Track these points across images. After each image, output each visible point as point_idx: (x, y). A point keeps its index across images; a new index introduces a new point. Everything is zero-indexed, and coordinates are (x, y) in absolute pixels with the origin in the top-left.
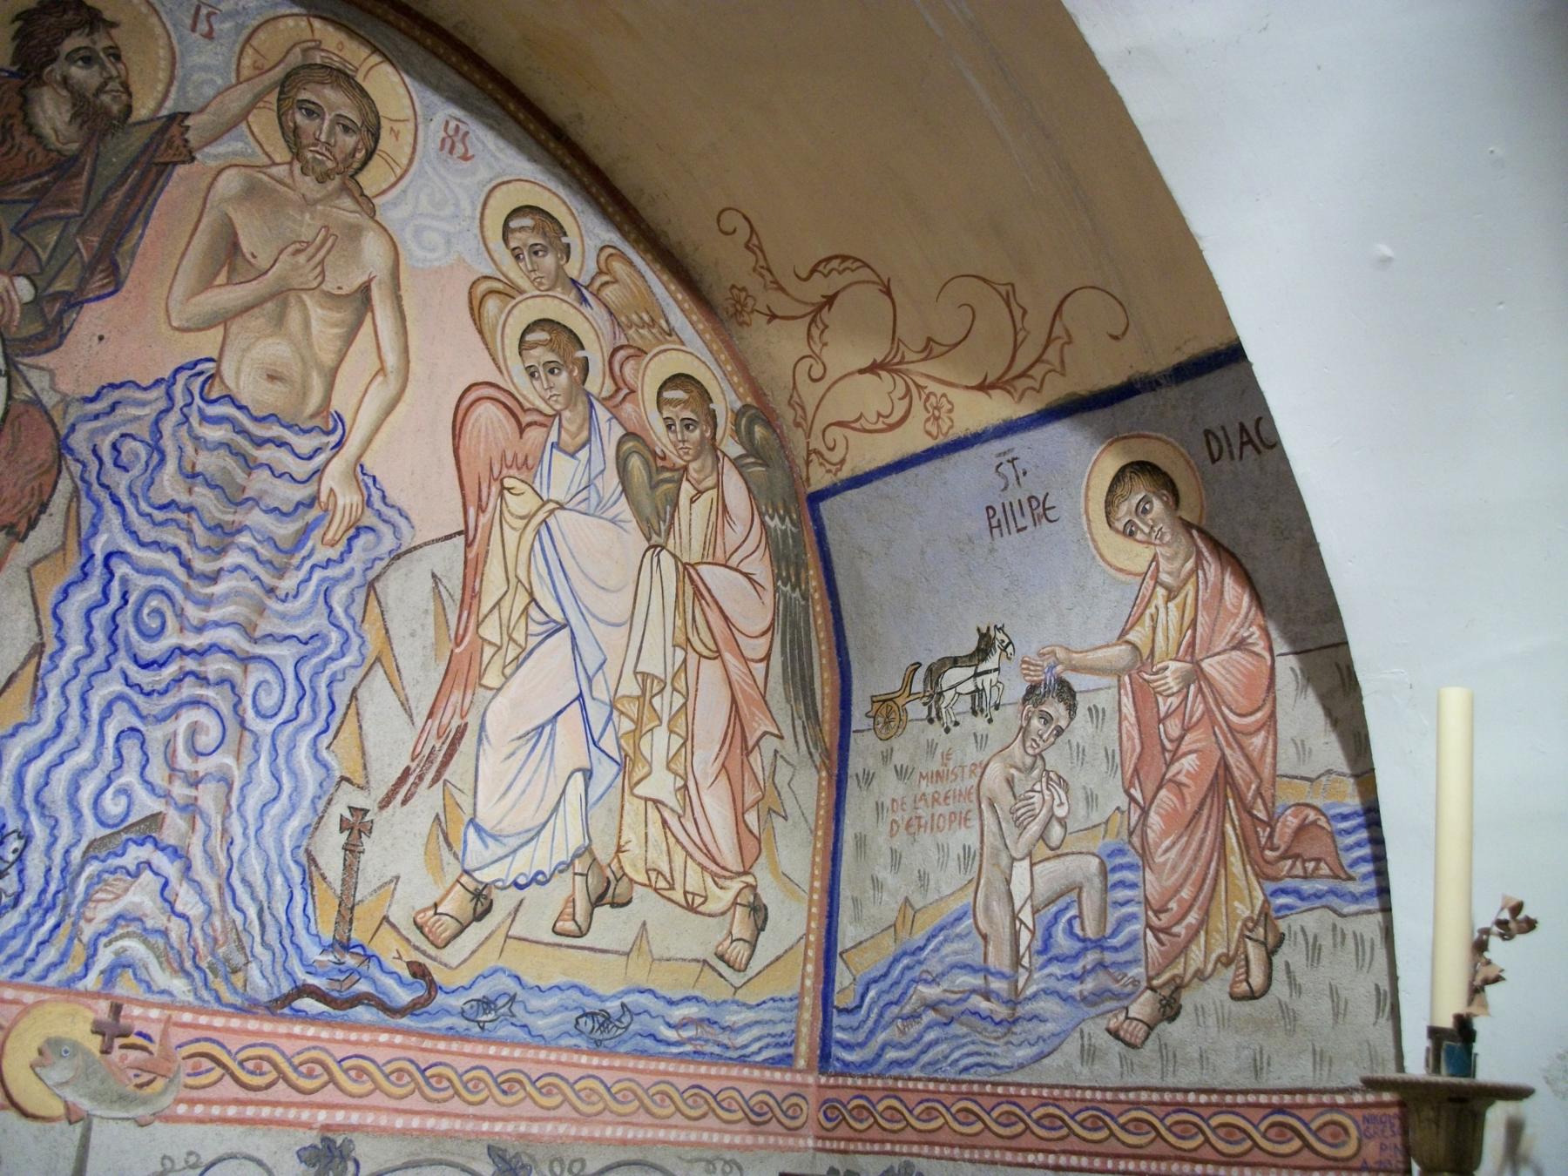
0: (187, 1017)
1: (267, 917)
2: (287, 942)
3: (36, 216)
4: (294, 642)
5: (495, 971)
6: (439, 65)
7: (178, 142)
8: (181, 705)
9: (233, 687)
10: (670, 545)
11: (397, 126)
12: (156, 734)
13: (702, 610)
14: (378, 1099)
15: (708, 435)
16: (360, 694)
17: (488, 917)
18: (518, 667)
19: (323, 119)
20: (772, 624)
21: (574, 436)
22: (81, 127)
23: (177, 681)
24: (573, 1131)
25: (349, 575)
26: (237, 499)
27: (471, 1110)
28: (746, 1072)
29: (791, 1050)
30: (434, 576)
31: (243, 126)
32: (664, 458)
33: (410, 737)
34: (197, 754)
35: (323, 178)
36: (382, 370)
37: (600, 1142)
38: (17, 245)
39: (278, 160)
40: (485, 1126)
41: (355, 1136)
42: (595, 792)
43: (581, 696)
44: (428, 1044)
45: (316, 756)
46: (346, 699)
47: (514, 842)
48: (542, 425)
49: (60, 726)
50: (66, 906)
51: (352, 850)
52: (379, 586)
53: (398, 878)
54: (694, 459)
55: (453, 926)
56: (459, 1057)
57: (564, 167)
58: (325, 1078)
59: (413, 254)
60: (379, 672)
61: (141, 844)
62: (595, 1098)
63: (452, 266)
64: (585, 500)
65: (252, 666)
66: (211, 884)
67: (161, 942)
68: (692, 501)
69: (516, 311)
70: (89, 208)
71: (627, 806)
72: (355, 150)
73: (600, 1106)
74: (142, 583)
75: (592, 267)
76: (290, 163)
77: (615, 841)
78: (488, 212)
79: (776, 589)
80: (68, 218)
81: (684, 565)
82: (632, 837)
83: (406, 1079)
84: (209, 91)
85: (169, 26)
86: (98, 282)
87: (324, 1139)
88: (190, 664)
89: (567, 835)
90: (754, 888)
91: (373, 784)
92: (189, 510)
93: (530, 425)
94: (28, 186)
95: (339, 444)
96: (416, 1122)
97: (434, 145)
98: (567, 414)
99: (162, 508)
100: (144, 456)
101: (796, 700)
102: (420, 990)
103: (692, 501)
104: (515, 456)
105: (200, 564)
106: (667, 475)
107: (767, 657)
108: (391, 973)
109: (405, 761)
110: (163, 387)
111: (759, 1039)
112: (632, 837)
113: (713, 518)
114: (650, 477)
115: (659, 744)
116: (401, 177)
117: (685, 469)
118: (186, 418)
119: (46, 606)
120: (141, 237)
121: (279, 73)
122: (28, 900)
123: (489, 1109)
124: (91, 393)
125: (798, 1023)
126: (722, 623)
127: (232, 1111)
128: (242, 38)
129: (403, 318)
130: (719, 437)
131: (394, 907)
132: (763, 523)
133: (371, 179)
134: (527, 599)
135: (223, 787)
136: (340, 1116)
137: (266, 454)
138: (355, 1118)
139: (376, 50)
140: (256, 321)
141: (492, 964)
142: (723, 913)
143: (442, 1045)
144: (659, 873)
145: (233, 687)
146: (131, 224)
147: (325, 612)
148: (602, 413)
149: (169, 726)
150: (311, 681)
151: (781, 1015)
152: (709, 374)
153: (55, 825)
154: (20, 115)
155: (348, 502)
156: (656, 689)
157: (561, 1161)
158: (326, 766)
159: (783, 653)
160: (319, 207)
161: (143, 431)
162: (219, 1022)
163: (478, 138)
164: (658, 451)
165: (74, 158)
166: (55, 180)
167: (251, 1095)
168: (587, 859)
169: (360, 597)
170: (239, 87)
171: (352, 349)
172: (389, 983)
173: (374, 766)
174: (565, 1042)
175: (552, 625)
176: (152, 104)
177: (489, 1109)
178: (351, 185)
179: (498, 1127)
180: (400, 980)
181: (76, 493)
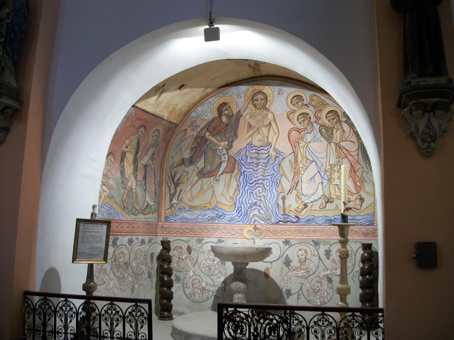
0: (264, 226)
1: (273, 212)
2: (276, 215)
4: (270, 176)
5: (309, 215)
6: (274, 81)
7: (240, 114)
8: (256, 188)
9: (263, 184)
10: (333, 141)
11: (270, 95)
12: (254, 192)
13: (342, 150)
14: (293, 234)
15: (338, 119)
16: (281, 180)
17: (307, 207)
20: (358, 148)
21: (310, 130)
23: (255, 185)
24: (327, 238)
25: (276, 164)
26: (258, 159)
27: (308, 235)
28: (362, 227)
29: (372, 222)
30: (289, 160)
31: (248, 108)
32: (329, 127)
33: (290, 184)
34: (260, 193)
36: (275, 133)
37: (332, 239)
39: (253, 110)
40: (311, 238)
41: (290, 240)
42: (324, 186)
43: (319, 171)
44: (299, 227)
45: (276, 190)
46: (279, 181)
47: (310, 196)
48: (304, 131)
49: (242, 194)
50: (247, 215)
51: (284, 202)
52: (281, 164)
53: (291, 204)
54: (336, 124)
55: (301, 210)
56: (306, 228)
57: (300, 85)
58: (285, 232)
59: (276, 113)
60: (283, 176)
61: (255, 206)
62: (331, 233)
63: (283, 112)
64: (315, 139)
65: (265, 180)
66: (265, 209)
67: (259, 217)
68: (336, 132)
69: (296, 114)
71: (331, 187)
72: (264, 102)
73: (332, 234)
74: (248, 174)
75: (309, 100)
77: (329, 192)
78: (288, 101)
79: (358, 141)
80: (229, 131)
81: (336, 144)
82: (332, 191)
83: (297, 232)
84: (242, 105)
87: (286, 240)
88: (256, 182)
89: (320, 193)
90: (360, 196)
91: (285, 192)
92: (252, 163)
93: (301, 132)
94: (224, 130)
95: (271, 146)
96: (299, 237)
97: (276, 95)
99: (249, 164)
101: (366, 160)
102: (297, 219)
105: (255, 169)
106: (330, 130)
107: (358, 155)
108: (292, 217)
109: (290, 188)
110: (245, 148)
111: (364, 221)
112: (332, 191)
113: (341, 133)
114: (326, 131)
115: (336, 175)
117: (334, 127)
118: (249, 151)
119: (238, 179)
121: (251, 97)
122: (243, 214)
123: (311, 235)
124: (237, 152)
125: (374, 218)
126: (346, 151)
127: (272, 237)
129: (277, 124)
130: (340, 119)
131: (291, 209)
132: (353, 130)
134: (306, 159)
135: (264, 197)
136: (287, 237)
137: (260, 152)
138: (290, 237)
139: (264, 85)
140: (255, 134)
141: (309, 214)
142: (354, 201)
143: (302, 227)
144: (339, 196)
145: (263, 184)
146: (237, 129)
148: (315, 124)
149: (255, 191)
151: (369, 217)
152: (336, 108)
153: (244, 205)
155: (274, 154)
156: (334, 166)
157: (325, 242)
158: (278, 191)
159: (362, 152)
161: (244, 155)
162: (269, 226)
163: (284, 90)
164: (327, 126)
165: (228, 124)
167: (275, 235)
168: (324, 196)
169: (278, 167)
172: (292, 219)
173: (285, 190)
174: (324, 224)
175: (311, 162)
176: (235, 111)
177: (311, 235)
178: (265, 108)
179: (313, 238)
180: (294, 218)
181: (238, 165)
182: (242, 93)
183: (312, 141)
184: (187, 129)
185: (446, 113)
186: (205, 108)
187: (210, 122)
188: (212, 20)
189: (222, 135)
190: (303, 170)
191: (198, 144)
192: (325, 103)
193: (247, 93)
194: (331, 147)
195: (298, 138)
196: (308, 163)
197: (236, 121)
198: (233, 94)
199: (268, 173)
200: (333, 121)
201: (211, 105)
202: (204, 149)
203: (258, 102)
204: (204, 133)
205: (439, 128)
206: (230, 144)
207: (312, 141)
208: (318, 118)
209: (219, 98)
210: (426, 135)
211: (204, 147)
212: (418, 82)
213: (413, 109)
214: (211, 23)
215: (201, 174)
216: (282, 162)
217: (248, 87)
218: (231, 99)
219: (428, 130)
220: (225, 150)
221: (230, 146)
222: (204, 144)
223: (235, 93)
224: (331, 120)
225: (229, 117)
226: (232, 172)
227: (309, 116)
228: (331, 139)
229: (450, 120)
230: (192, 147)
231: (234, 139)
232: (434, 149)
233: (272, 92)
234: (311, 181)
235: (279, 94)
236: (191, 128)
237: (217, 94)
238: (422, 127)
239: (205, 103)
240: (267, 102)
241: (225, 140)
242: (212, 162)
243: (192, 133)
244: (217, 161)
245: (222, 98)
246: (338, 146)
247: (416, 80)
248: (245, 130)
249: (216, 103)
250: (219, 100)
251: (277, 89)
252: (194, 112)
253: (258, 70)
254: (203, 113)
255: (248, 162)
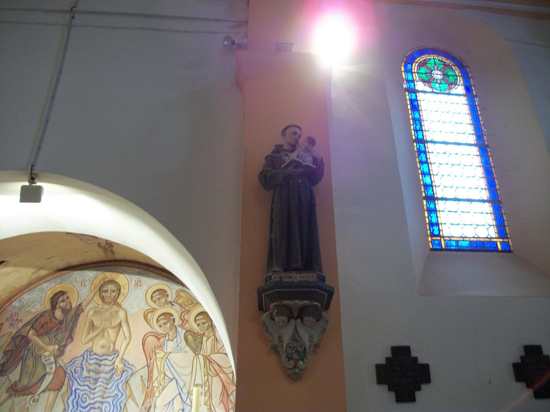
3: (57, 333)
7: (81, 309)
11: (124, 286)
15: (210, 323)
16: (126, 404)
18: (163, 390)
19: (108, 292)
21: (172, 336)
22: (63, 314)
25: (122, 381)
31: (93, 301)
35: (109, 304)
36: (125, 338)
38: (55, 339)
39: (100, 304)
43: (180, 393)
46: (124, 405)
48: (164, 337)
52: (129, 382)
54: (206, 331)
57: (166, 277)
59: (130, 311)
60: (130, 399)
68: (206, 341)
69: (155, 314)
70: (66, 328)
74: (82, 393)
75: (174, 296)
76: (103, 304)
78: (147, 295)
80: (63, 332)
81: (206, 357)
84: (85, 297)
85: (77, 288)
86: (69, 340)
88: (92, 406)
92: (89, 377)
93: (161, 338)
94: (55, 328)
95: (118, 356)
97: (133, 286)
98: (170, 332)
99: (84, 378)
100: (80, 370)
103: (206, 341)
104: (158, 346)
105: (92, 387)
116: (126, 296)
117: (204, 334)
118: (87, 360)
120: (76, 330)
124: (69, 361)
128: (91, 283)
133: (119, 301)
134: (164, 375)
137: (102, 363)
139: (118, 272)
140: (99, 338)
145: (101, 408)
147: (118, 390)
148: (179, 329)
150: (116, 404)
154: (53, 316)
155: (121, 366)
160: (109, 310)
163: (143, 280)
164: (196, 332)
165: (63, 320)
166: (60, 326)
169: (125, 385)
170: (91, 293)
171: (119, 336)
175: (170, 379)
178: (115, 303)
181: (69, 381)
182: (88, 280)
183: (173, 352)
184: (3, 323)
185: (317, 321)
186: (34, 296)
187: (38, 316)
188: (33, 176)
189: (52, 335)
190: (158, 390)
191: (16, 347)
192: (195, 302)
193: (95, 281)
194: (198, 361)
195: (155, 346)
196: (166, 381)
197: (74, 318)
198: (75, 281)
199: (109, 393)
200: (203, 325)
201: (43, 293)
202: (23, 354)
203: (108, 294)
204: (28, 331)
205: (310, 341)
206: (61, 349)
207: (173, 352)
208: (184, 321)
209: (56, 284)
210: (292, 350)
211: (23, 351)
212: (281, 278)
213: (274, 313)
214: (32, 179)
215: (13, 390)
216: (131, 378)
217: (97, 273)
218: (72, 287)
219: (294, 343)
220: (53, 357)
221: (61, 352)
222: (24, 346)
223: (78, 280)
224: (201, 325)
225: (65, 311)
226: (59, 390)
227: (172, 318)
228: (199, 349)
229: (324, 330)
230: (6, 350)
231: (68, 342)
232: (302, 370)
233: (127, 282)
234: (167, 407)
235: (137, 286)
236: (9, 323)
237: (54, 278)
238: (286, 339)
239: (35, 289)
240: (119, 295)
241: (55, 343)
242: (31, 374)
243: (10, 330)
244: (40, 372)
245: (59, 285)
246: (208, 359)
247: (278, 275)
248: (84, 331)
249: (50, 290)
250: (55, 287)
251: (134, 278)
252: (17, 300)
253: (111, 253)
254: (31, 303)
255: (83, 376)
